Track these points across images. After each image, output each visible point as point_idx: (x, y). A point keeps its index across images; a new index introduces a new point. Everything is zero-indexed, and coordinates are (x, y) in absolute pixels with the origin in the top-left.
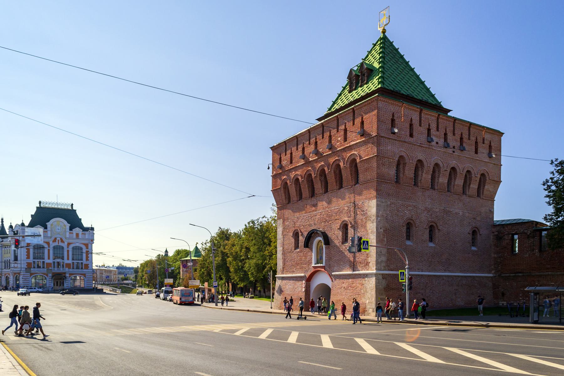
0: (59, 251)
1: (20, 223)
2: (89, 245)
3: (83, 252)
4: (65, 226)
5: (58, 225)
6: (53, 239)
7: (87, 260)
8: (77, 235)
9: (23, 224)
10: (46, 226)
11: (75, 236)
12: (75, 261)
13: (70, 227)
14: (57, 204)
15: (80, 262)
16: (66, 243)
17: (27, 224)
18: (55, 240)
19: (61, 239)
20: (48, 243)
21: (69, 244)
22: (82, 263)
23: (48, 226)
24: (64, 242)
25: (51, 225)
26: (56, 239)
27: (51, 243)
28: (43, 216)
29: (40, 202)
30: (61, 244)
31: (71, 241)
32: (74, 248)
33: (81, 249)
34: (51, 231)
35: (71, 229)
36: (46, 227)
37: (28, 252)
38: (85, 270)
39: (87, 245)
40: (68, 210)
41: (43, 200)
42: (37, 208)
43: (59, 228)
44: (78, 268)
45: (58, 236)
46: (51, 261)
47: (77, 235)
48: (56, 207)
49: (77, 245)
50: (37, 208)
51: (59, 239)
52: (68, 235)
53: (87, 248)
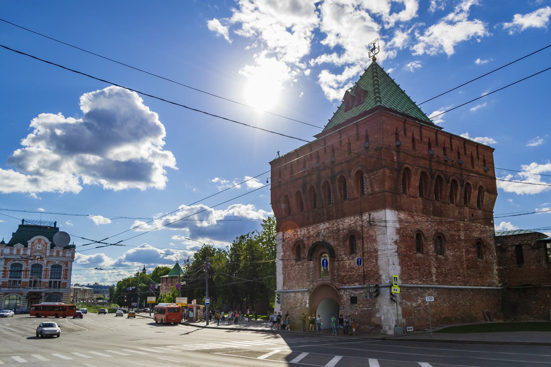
0: (37, 269)
2: (69, 263)
3: (61, 271)
4: (46, 244)
5: (39, 243)
7: (66, 278)
8: (58, 252)
11: (55, 254)
12: (53, 280)
15: (58, 280)
16: (45, 262)
17: (7, 242)
22: (60, 282)
23: (30, 244)
25: (33, 243)
28: (25, 233)
29: (23, 221)
30: (39, 262)
31: (50, 259)
32: (52, 267)
33: (61, 267)
34: (31, 249)
36: (26, 246)
38: (62, 289)
39: (66, 263)
40: (51, 228)
42: (20, 226)
43: (40, 246)
44: (55, 287)
45: (38, 254)
46: (28, 280)
47: (58, 252)
49: (57, 262)
50: (20, 226)
53: (67, 266)
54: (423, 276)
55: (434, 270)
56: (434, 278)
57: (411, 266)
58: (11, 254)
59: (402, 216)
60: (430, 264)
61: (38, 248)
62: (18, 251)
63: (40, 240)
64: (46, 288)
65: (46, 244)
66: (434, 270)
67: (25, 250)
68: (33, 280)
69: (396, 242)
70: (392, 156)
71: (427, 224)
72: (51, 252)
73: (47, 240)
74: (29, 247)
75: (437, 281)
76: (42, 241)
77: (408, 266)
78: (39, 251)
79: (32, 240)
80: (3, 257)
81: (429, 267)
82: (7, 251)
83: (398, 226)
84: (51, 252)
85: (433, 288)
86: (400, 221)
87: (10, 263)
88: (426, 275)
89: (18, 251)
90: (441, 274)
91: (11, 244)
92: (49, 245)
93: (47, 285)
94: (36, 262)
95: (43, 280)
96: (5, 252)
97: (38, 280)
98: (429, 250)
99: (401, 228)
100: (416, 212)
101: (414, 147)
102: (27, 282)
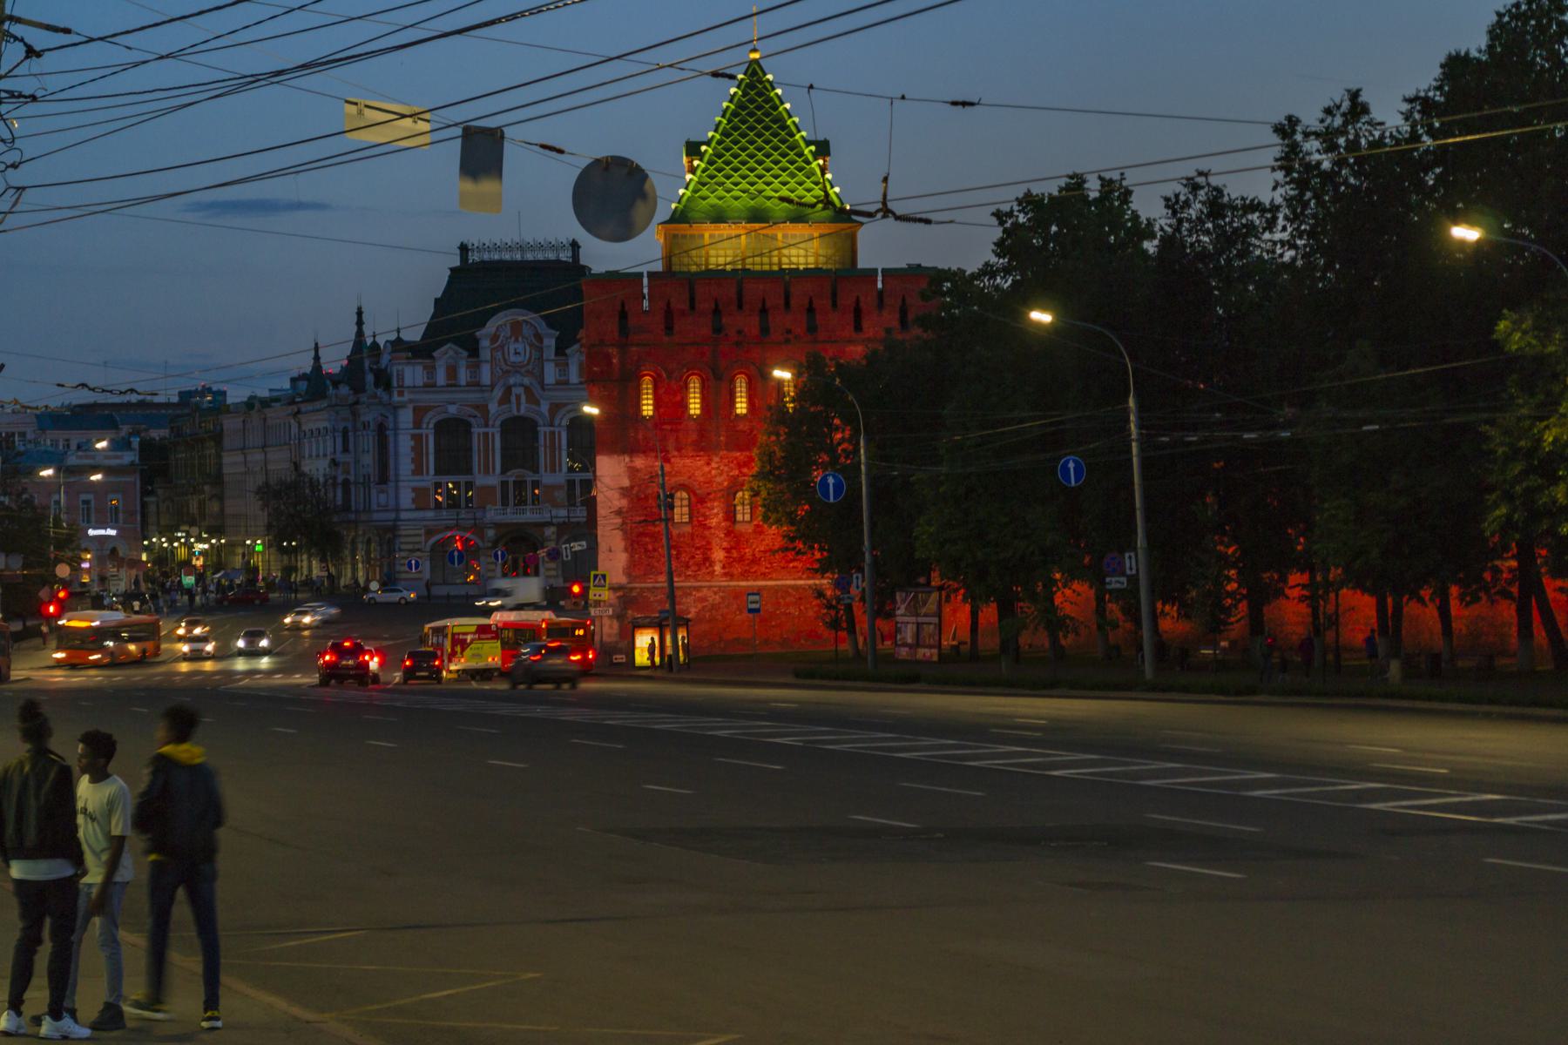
1: (393, 337)
6: (498, 393)
9: (398, 345)
10: (477, 341)
13: (558, 339)
14: (521, 248)
16: (545, 408)
18: (505, 399)
19: (527, 389)
20: (483, 408)
21: (555, 408)
23: (485, 343)
24: (538, 403)
25: (494, 338)
26: (508, 390)
27: (493, 408)
29: (464, 249)
30: (524, 409)
35: (560, 350)
36: (473, 350)
37: (417, 438)
41: (473, 239)
42: (452, 270)
43: (520, 349)
46: (493, 480)
48: (518, 257)
51: (520, 390)
52: (551, 374)
54: (688, 567)
55: (719, 555)
56: (718, 568)
57: (655, 550)
58: (430, 386)
59: (639, 462)
60: (709, 543)
61: (513, 358)
62: (452, 372)
63: (516, 328)
64: (556, 505)
65: (539, 338)
66: (719, 555)
67: (475, 367)
68: (511, 480)
69: (619, 512)
70: (608, 357)
71: (706, 469)
72: (563, 367)
73: (542, 327)
74: (485, 354)
75: (725, 574)
76: (526, 330)
77: (646, 550)
78: (516, 369)
79: (491, 326)
80: (407, 397)
81: (707, 548)
82: (413, 374)
83: (626, 483)
84: (563, 367)
85: (710, 587)
86: (633, 472)
87: (430, 421)
88: (698, 565)
89: (452, 372)
90: (741, 559)
91: (421, 351)
92: (550, 343)
93: (561, 495)
94: (515, 412)
95: (547, 479)
96: (408, 381)
97: (530, 477)
98: (706, 517)
99: (632, 487)
100: (679, 449)
101: (669, 328)
102: (494, 488)
